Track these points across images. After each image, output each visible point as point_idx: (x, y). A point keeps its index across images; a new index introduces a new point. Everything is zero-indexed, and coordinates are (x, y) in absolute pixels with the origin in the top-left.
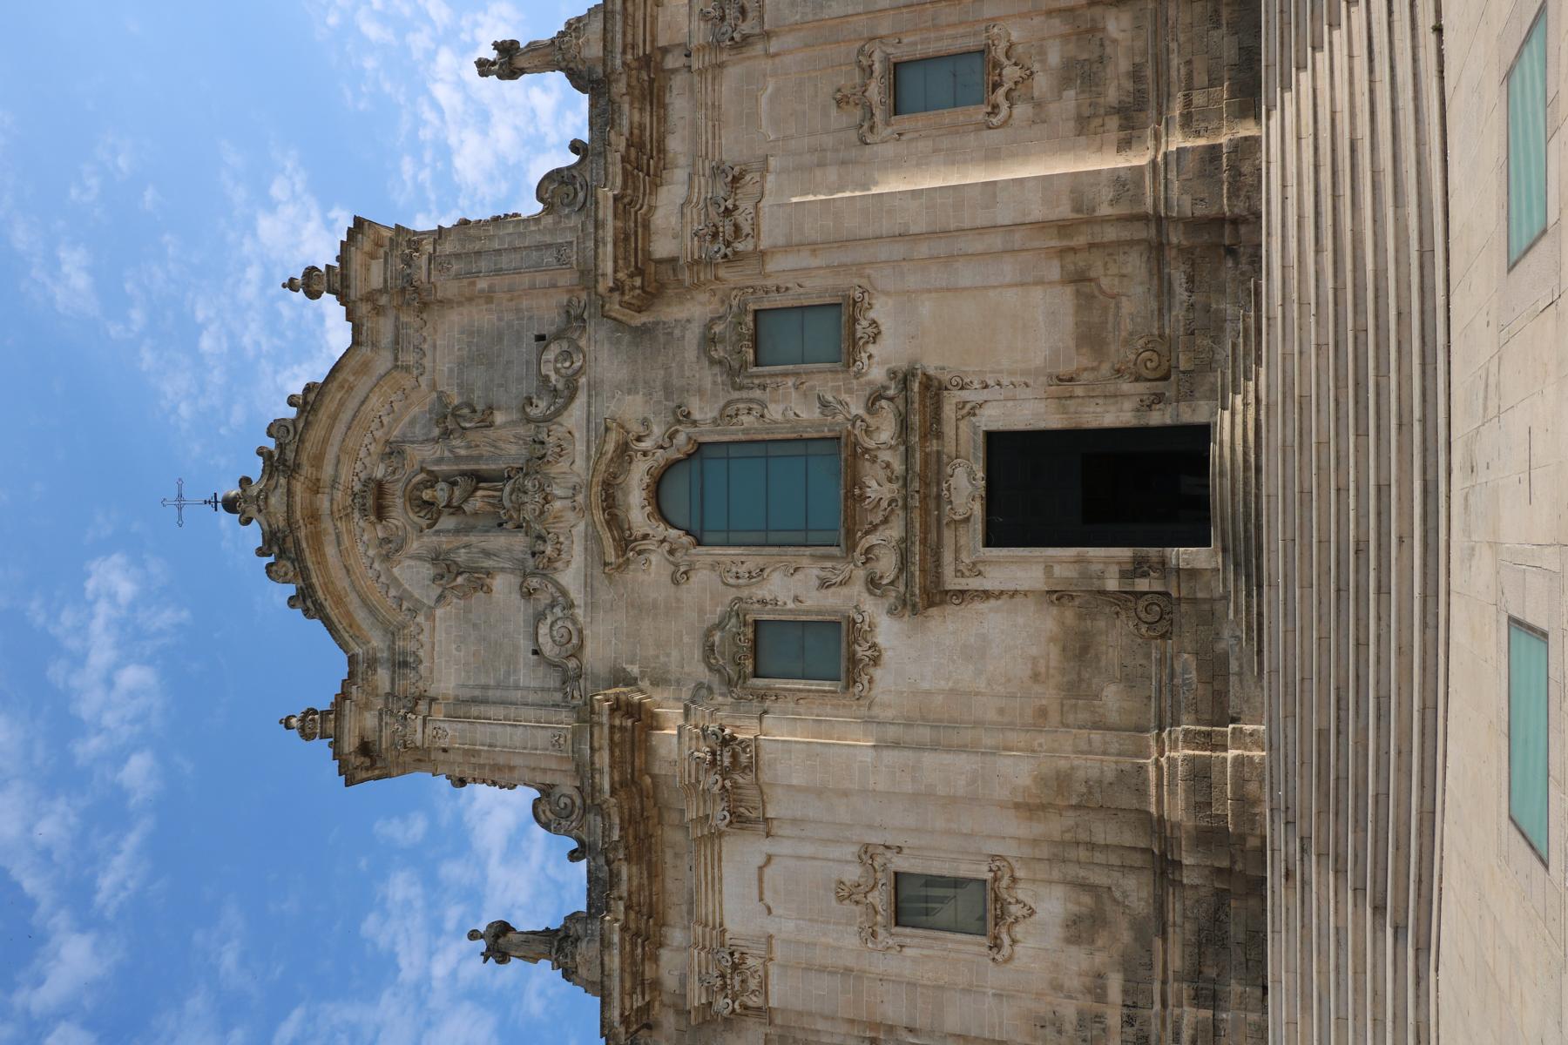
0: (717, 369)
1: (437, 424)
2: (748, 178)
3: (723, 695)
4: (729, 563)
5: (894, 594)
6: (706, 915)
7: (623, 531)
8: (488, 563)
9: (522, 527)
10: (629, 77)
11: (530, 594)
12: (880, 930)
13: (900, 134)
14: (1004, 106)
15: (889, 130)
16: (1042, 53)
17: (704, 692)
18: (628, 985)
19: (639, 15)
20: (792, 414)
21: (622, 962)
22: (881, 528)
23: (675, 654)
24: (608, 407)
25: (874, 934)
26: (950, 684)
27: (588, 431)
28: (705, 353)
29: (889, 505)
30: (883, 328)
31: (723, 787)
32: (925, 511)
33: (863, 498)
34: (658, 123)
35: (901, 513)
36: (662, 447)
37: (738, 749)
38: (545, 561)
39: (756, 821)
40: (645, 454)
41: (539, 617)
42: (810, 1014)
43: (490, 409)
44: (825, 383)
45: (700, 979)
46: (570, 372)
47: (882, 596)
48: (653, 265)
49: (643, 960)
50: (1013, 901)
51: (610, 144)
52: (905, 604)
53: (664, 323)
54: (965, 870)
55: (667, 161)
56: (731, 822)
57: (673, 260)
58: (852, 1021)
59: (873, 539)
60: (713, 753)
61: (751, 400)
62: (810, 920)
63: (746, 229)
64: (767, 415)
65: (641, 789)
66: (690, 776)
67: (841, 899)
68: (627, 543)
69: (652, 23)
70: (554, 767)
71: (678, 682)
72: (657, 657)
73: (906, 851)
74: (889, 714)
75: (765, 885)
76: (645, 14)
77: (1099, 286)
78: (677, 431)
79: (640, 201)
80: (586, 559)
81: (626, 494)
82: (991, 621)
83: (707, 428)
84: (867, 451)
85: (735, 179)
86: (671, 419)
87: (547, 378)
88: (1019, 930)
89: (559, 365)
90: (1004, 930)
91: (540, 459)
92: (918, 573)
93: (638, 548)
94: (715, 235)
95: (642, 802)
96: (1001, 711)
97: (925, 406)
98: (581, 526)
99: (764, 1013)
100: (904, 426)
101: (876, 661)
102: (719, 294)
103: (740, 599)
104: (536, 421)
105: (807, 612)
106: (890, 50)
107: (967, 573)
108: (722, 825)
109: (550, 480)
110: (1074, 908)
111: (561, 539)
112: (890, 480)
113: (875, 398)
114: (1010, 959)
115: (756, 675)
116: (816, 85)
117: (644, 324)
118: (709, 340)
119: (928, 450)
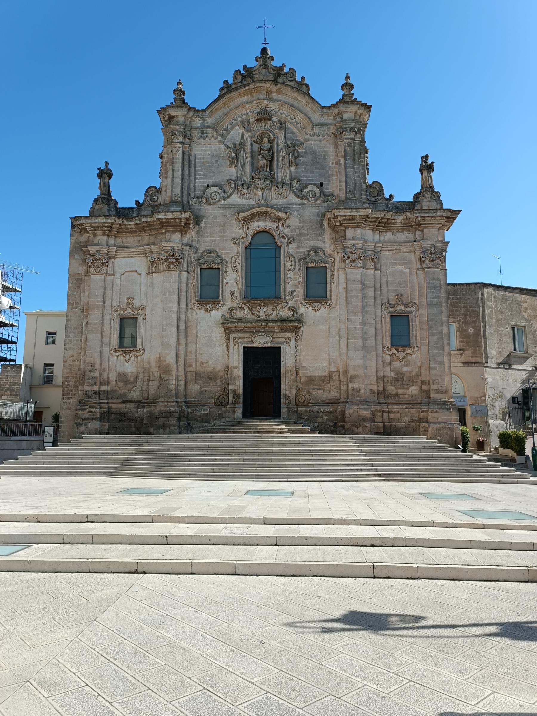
0: (306, 253)
1: (291, 143)
2: (373, 264)
3: (194, 256)
4: (239, 259)
5: (228, 317)
6: (119, 252)
7: (250, 219)
8: (240, 166)
9: (253, 179)
10: (413, 219)
11: (229, 184)
12: (118, 313)
13: (384, 317)
14: (390, 353)
15: (386, 314)
16: (408, 365)
17: (195, 250)
18: (94, 225)
19: (435, 222)
20: (290, 281)
21: (101, 223)
22: (250, 312)
23: (208, 239)
24: (295, 212)
25: (117, 311)
26: (199, 336)
27: (287, 205)
28: (313, 248)
29: (258, 315)
30: (317, 312)
31: (162, 259)
32: (255, 328)
33: (260, 306)
34: (397, 229)
35: (256, 319)
36: (279, 233)
37: (175, 264)
38: (240, 189)
39: (152, 269)
40: (277, 227)
41: (221, 187)
42: (90, 289)
43: (297, 165)
44: (301, 292)
45: (98, 251)
46: (309, 197)
47: (228, 313)
48: (344, 229)
49: (103, 230)
50: (130, 356)
51: (388, 212)
52: (226, 320)
53: (324, 233)
54: (139, 341)
55: (383, 233)
56: (151, 261)
57: (344, 237)
58: (88, 304)
59: (246, 309)
60: (173, 256)
61: (295, 266)
62: (120, 289)
63: (353, 264)
64: (289, 272)
65: (160, 229)
66: (165, 247)
67: (127, 299)
68: (246, 221)
69: (433, 226)
70: (167, 195)
71: (198, 241)
72: (207, 233)
73: (144, 321)
74: (189, 316)
75: (131, 273)
76: (436, 224)
77: (327, 383)
78: (285, 239)
79: (367, 224)
80: (241, 205)
81: (263, 220)
82: (220, 348)
83: (286, 250)
84: (276, 307)
85: (372, 259)
86: (289, 236)
87: (307, 188)
88: (122, 357)
89: (311, 193)
90: (121, 353)
91: (277, 186)
92: (235, 325)
93: (244, 225)
94: (352, 253)
95: (156, 229)
96: (191, 352)
97: (290, 327)
98: (253, 203)
99: (88, 273)
100: (284, 320)
101: (206, 311)
102: (333, 254)
103: (227, 263)
104: (291, 184)
105: (222, 287)
106: (414, 314)
107: (235, 341)
108: (149, 258)
109: (270, 190)
110: (129, 375)
111: (248, 195)
112: (266, 315)
113: (293, 310)
114: (113, 355)
115: (201, 269)
116: (404, 287)
117: (324, 225)
118: (316, 250)
119: (275, 328)
